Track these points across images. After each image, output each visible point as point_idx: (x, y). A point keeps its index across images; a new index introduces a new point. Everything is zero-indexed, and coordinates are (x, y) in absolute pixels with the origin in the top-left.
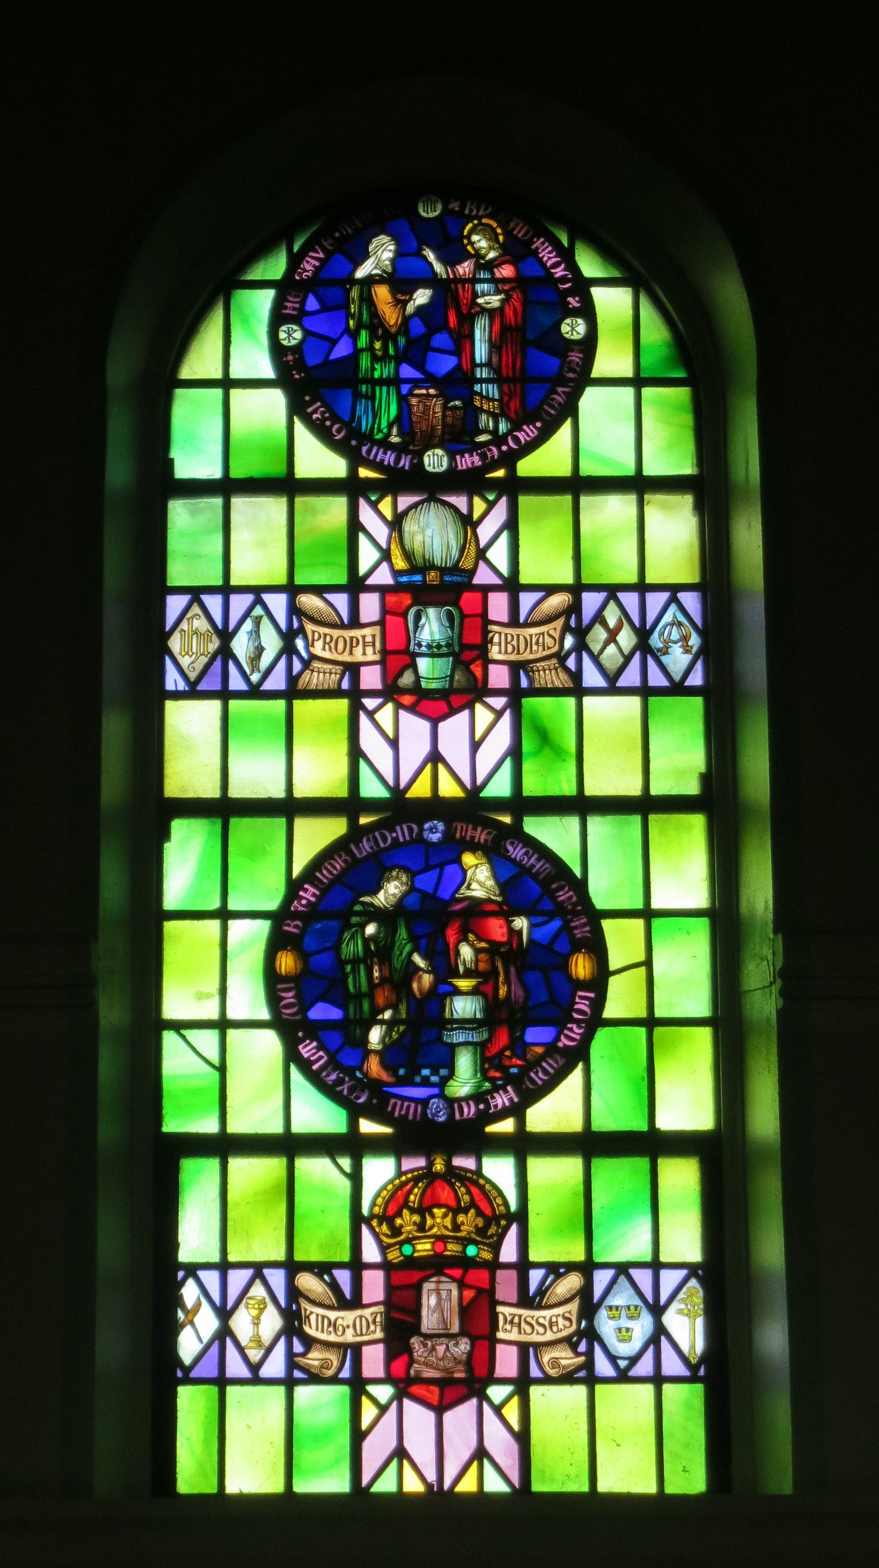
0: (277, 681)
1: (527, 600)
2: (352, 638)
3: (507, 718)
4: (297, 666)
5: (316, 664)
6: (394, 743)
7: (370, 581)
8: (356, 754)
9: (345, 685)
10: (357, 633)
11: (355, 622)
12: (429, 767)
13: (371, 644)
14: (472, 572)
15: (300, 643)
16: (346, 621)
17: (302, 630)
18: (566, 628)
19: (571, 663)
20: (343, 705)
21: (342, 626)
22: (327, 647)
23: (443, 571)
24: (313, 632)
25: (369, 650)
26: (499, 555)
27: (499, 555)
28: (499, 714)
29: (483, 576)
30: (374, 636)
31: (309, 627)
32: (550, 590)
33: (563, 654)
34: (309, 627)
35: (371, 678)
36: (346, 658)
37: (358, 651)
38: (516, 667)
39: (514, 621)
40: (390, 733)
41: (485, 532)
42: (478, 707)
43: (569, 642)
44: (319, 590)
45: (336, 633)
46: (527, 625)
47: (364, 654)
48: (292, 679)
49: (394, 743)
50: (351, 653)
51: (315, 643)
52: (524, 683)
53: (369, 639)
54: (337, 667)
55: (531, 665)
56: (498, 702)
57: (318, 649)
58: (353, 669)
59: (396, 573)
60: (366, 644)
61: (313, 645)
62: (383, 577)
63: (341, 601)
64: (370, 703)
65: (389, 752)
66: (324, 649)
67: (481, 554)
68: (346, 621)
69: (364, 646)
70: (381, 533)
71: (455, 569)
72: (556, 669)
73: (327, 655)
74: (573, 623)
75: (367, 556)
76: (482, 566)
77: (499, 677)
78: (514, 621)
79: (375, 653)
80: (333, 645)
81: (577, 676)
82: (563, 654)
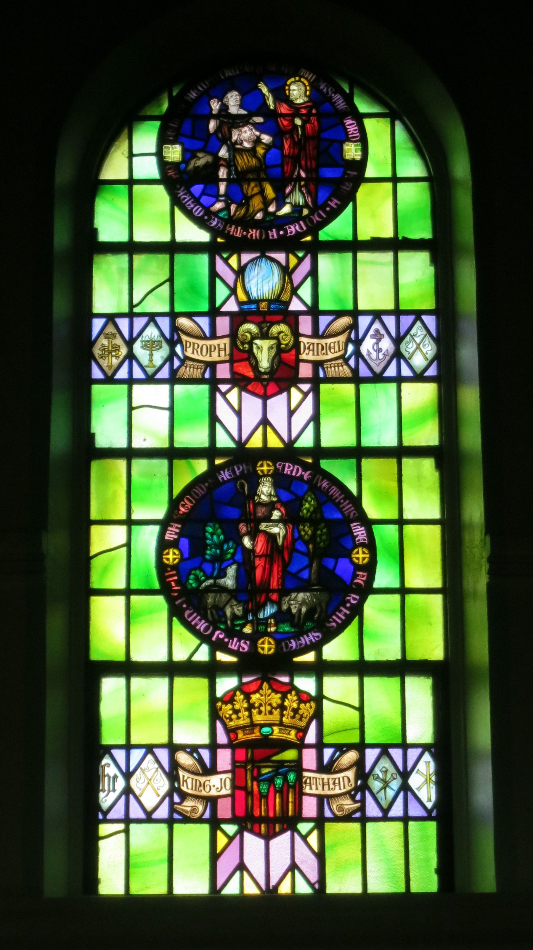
0: (164, 373)
1: (324, 321)
2: (211, 346)
3: (310, 397)
4: (177, 363)
5: (188, 362)
6: (238, 413)
7: (224, 309)
8: (214, 419)
9: (207, 376)
10: (215, 342)
11: (214, 336)
12: (260, 429)
13: (223, 349)
14: (288, 303)
15: (178, 349)
16: (208, 334)
17: (180, 341)
18: (349, 340)
19: (352, 362)
20: (205, 389)
21: (205, 338)
22: (195, 351)
23: (270, 302)
24: (186, 342)
25: (222, 353)
26: (305, 292)
27: (305, 292)
28: (306, 395)
29: (295, 306)
30: (225, 345)
31: (184, 338)
32: (338, 314)
33: (346, 356)
34: (184, 338)
35: (223, 371)
36: (208, 359)
37: (215, 355)
38: (317, 365)
39: (316, 334)
40: (236, 407)
41: (297, 277)
42: (293, 390)
43: (351, 348)
44: (190, 315)
45: (201, 342)
46: (323, 337)
47: (219, 355)
48: (173, 372)
49: (238, 413)
50: (211, 356)
51: (188, 349)
52: (321, 375)
53: (222, 346)
54: (201, 365)
55: (326, 364)
56: (305, 387)
57: (189, 353)
58: (212, 366)
59: (240, 304)
60: (220, 349)
61: (186, 351)
62: (232, 306)
63: (204, 322)
64: (224, 388)
65: (235, 418)
66: (193, 353)
67: (294, 291)
68: (208, 334)
69: (219, 350)
70: (230, 278)
71: (277, 300)
72: (342, 366)
73: (195, 356)
74: (353, 336)
75: (222, 292)
76: (295, 300)
77: (305, 371)
78: (316, 334)
79: (226, 355)
80: (199, 350)
81: (355, 371)
82: (346, 356)
